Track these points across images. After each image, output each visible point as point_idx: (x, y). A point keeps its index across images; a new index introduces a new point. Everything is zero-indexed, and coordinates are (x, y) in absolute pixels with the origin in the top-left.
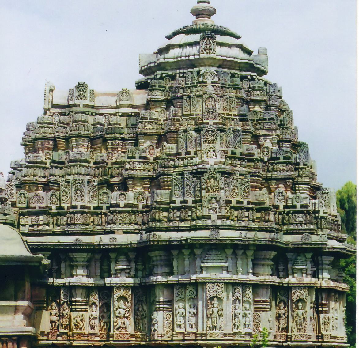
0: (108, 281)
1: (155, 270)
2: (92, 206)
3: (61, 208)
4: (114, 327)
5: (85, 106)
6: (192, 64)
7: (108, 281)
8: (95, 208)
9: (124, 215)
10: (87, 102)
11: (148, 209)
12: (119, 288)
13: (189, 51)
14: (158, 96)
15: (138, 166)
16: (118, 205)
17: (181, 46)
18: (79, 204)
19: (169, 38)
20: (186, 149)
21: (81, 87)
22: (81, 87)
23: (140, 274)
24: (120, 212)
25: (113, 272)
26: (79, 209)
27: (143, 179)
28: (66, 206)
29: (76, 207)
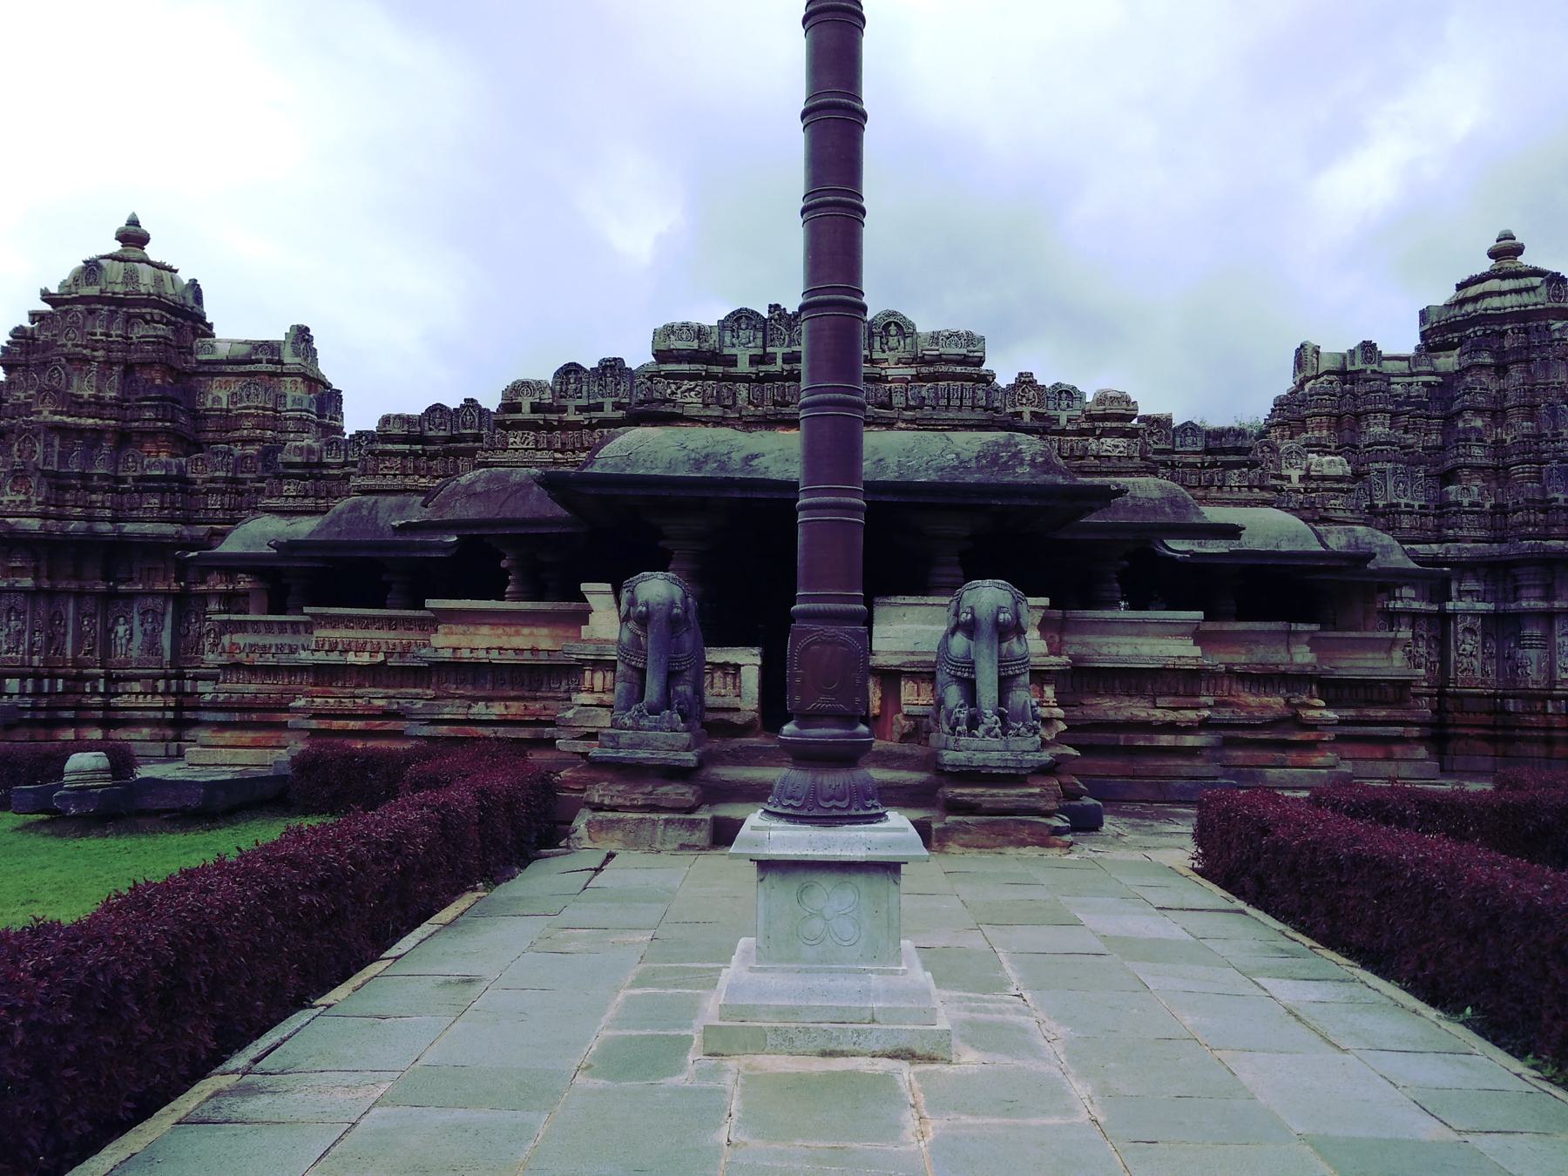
0: (1450, 606)
1: (1524, 592)
2: (1416, 504)
3: (1372, 507)
4: (1456, 669)
5: (1374, 372)
6: (1522, 316)
7: (1450, 606)
8: (1421, 507)
9: (1471, 517)
10: (1375, 367)
11: (1499, 509)
12: (1465, 614)
13: (1526, 298)
14: (1486, 359)
15: (1477, 451)
16: (1459, 504)
17: (1501, 294)
18: (1403, 501)
19: (1460, 287)
20: (1555, 428)
21: (1368, 348)
22: (1368, 348)
23: (1488, 597)
24: (1465, 513)
25: (1454, 594)
26: (1403, 508)
27: (1480, 468)
28: (1381, 504)
29: (1398, 505)
